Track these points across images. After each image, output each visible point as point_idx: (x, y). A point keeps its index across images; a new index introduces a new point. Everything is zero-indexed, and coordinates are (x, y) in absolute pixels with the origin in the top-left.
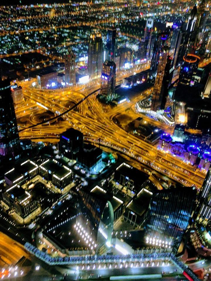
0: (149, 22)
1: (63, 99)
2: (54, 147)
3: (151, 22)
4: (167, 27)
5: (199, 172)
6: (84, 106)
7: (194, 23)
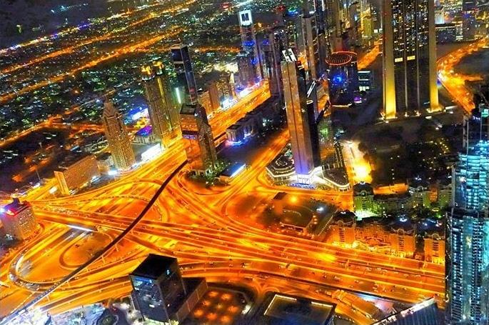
0: (243, 15)
1: (119, 202)
2: (124, 306)
3: (247, 14)
5: (429, 267)
6: (164, 204)
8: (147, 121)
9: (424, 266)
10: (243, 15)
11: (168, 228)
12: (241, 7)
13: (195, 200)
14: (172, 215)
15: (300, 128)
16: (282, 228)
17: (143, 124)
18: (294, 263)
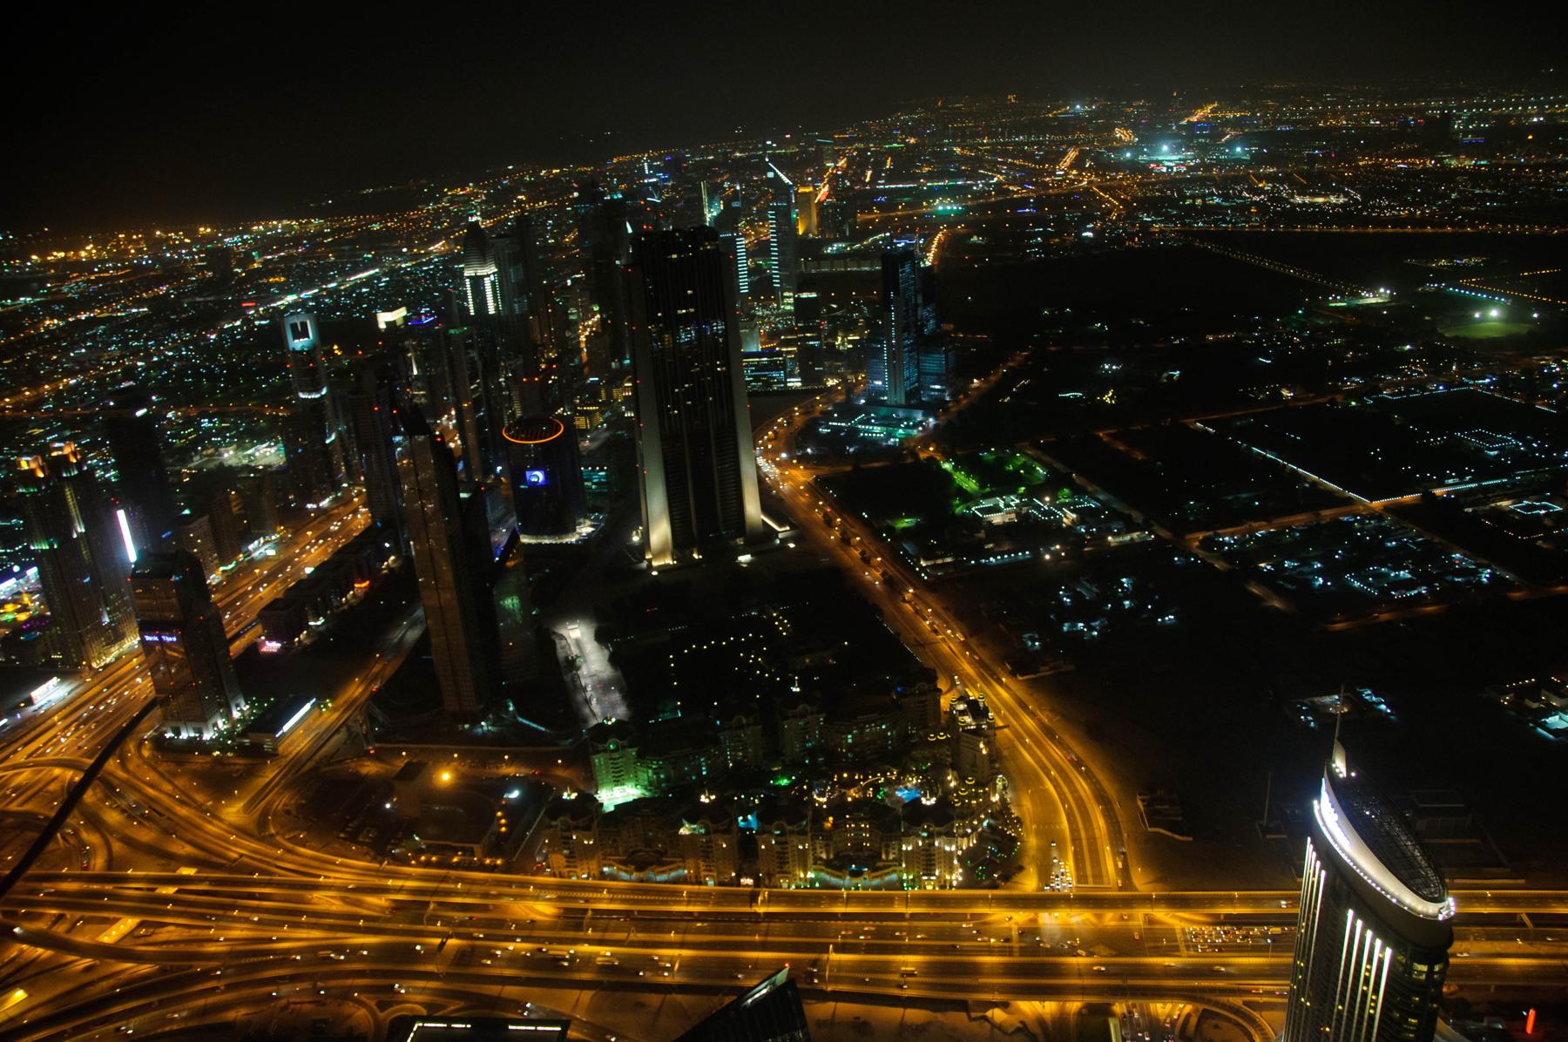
0: (294, 326)
3: (304, 325)
4: (382, 326)
5: (773, 899)
6: (95, 823)
7: (493, 283)
8: (34, 603)
9: (760, 899)
10: (294, 326)
11: (109, 887)
12: (290, 306)
13: (181, 802)
14: (117, 846)
15: (448, 596)
16: (422, 852)
17: (24, 609)
18: (458, 936)
